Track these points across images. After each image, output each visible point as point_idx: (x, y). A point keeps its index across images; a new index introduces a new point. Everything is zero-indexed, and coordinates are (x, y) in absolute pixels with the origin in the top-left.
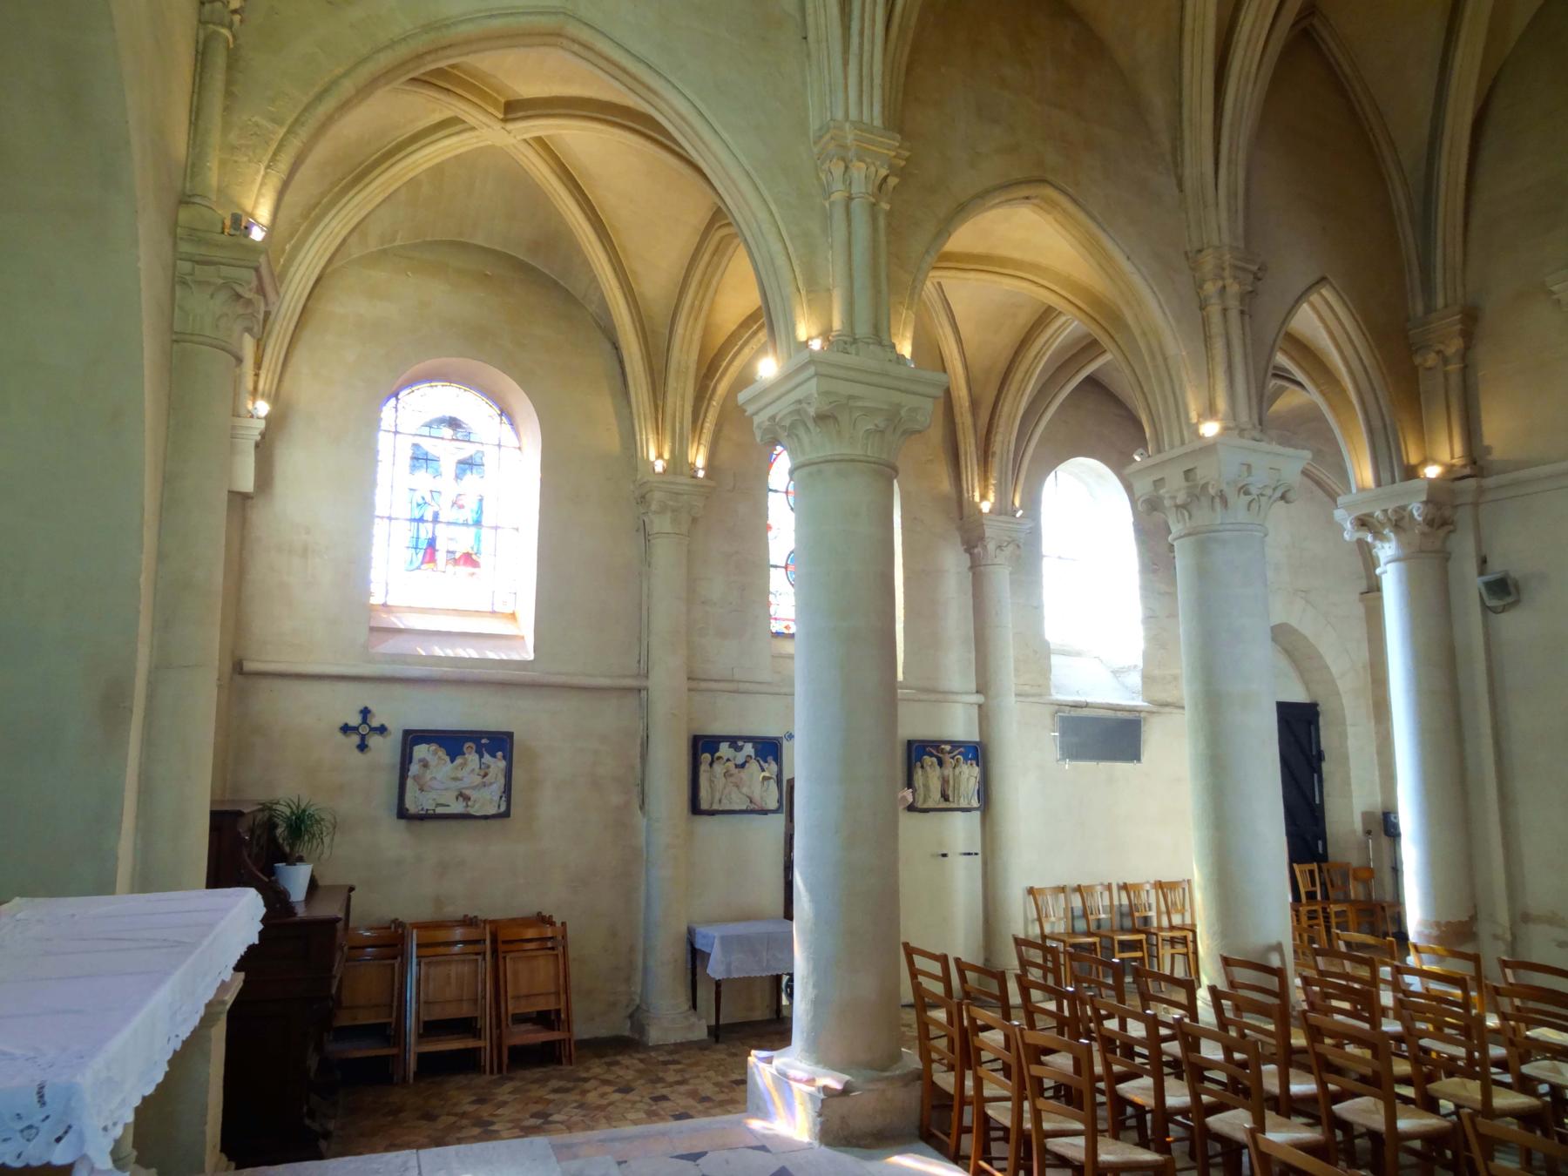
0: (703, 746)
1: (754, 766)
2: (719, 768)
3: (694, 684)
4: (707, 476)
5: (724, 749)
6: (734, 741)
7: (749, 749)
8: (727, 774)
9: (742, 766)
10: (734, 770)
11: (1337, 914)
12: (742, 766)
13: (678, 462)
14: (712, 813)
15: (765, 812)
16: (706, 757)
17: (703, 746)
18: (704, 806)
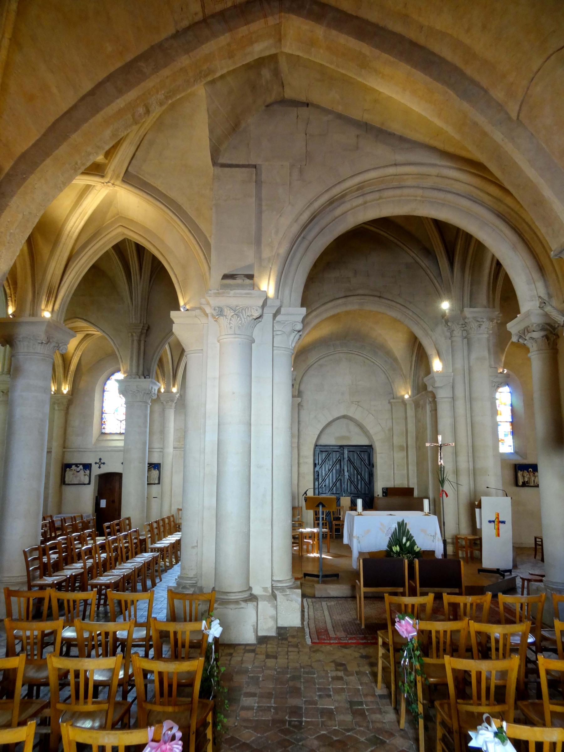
0: (66, 467)
1: (82, 472)
2: (71, 473)
3: (64, 450)
4: (55, 394)
5: (73, 466)
6: (77, 465)
7: (81, 467)
8: (73, 474)
9: (79, 472)
10: (76, 473)
11: (336, 525)
12: (79, 472)
13: (59, 390)
14: (69, 484)
15: (85, 484)
16: (68, 469)
17: (66, 467)
18: (66, 483)
